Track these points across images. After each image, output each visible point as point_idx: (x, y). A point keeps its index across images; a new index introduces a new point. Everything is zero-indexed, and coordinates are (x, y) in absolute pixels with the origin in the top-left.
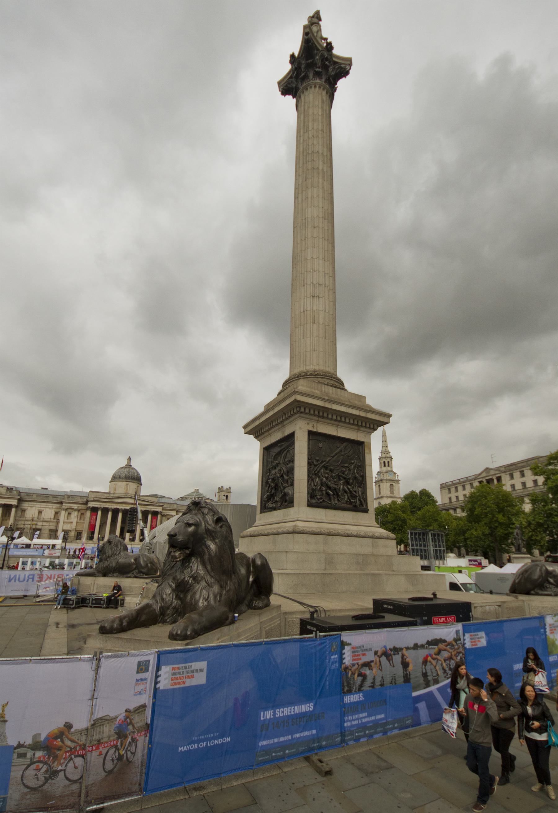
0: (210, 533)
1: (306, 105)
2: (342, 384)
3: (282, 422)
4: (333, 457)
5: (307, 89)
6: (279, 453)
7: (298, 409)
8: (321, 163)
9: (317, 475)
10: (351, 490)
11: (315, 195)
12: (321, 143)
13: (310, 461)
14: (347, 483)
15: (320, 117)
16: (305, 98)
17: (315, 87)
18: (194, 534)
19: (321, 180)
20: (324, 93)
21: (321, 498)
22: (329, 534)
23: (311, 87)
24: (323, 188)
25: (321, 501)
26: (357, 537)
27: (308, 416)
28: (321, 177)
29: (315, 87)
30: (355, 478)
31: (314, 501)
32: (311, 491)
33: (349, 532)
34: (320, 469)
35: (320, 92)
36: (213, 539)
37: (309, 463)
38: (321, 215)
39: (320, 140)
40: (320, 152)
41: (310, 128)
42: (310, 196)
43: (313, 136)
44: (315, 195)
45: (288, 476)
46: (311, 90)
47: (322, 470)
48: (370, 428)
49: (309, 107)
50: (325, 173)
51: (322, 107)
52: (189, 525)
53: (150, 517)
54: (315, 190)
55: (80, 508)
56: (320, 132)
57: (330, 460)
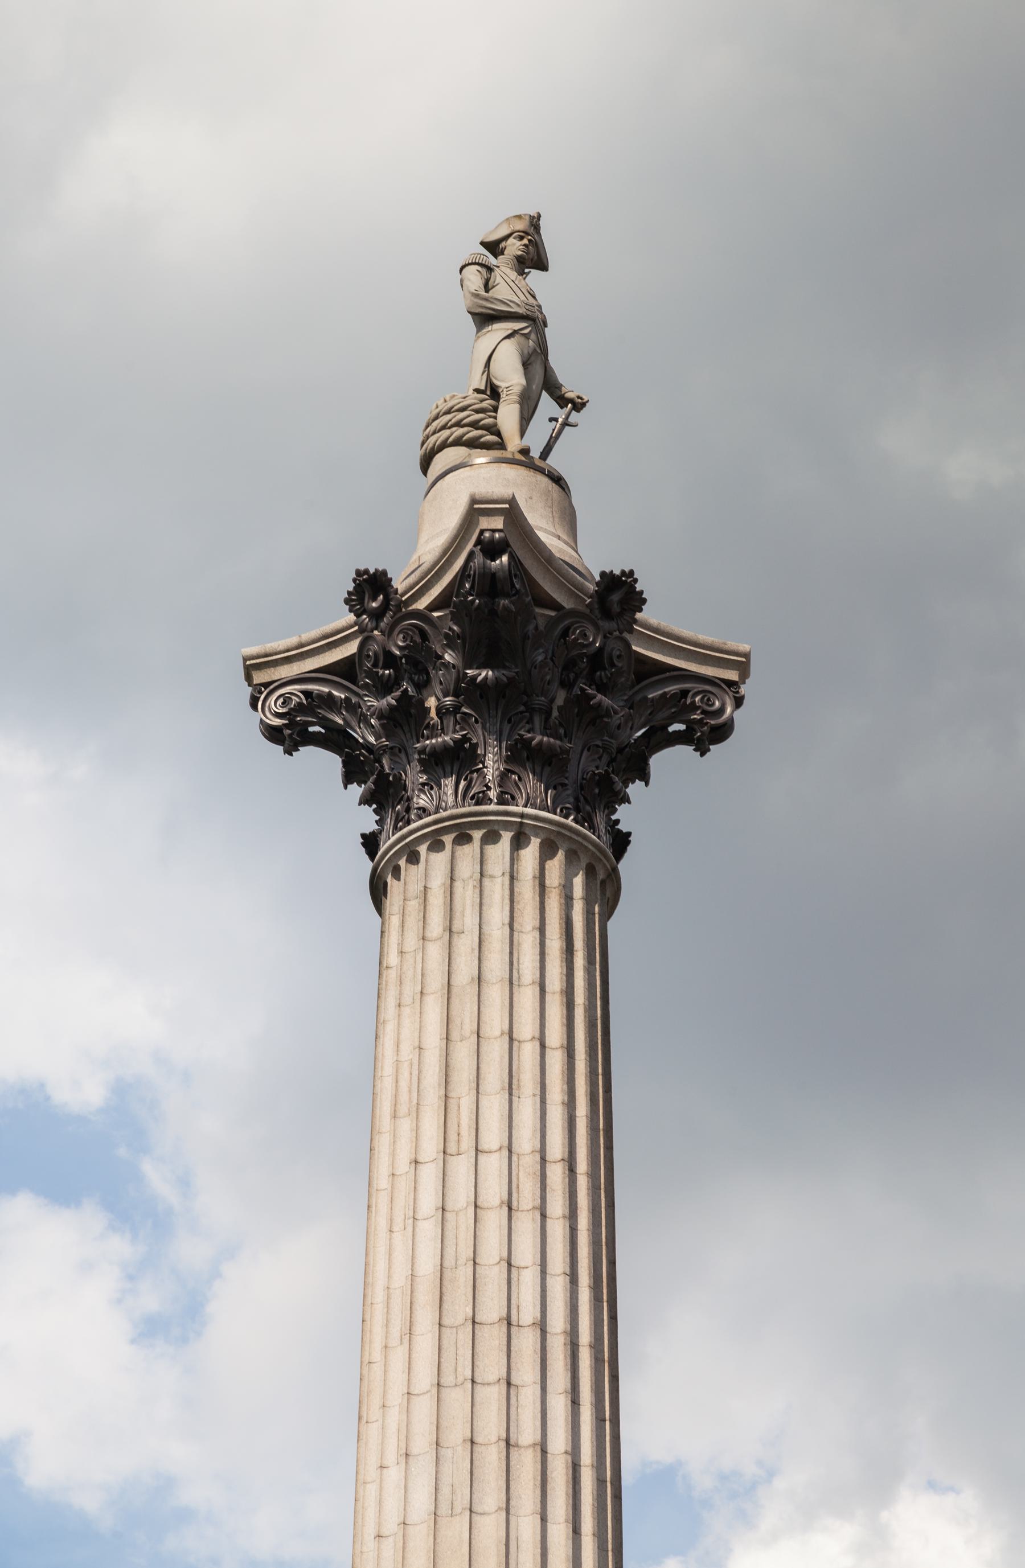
5: (463, 838)
17: (519, 842)
23: (492, 837)
29: (519, 842)
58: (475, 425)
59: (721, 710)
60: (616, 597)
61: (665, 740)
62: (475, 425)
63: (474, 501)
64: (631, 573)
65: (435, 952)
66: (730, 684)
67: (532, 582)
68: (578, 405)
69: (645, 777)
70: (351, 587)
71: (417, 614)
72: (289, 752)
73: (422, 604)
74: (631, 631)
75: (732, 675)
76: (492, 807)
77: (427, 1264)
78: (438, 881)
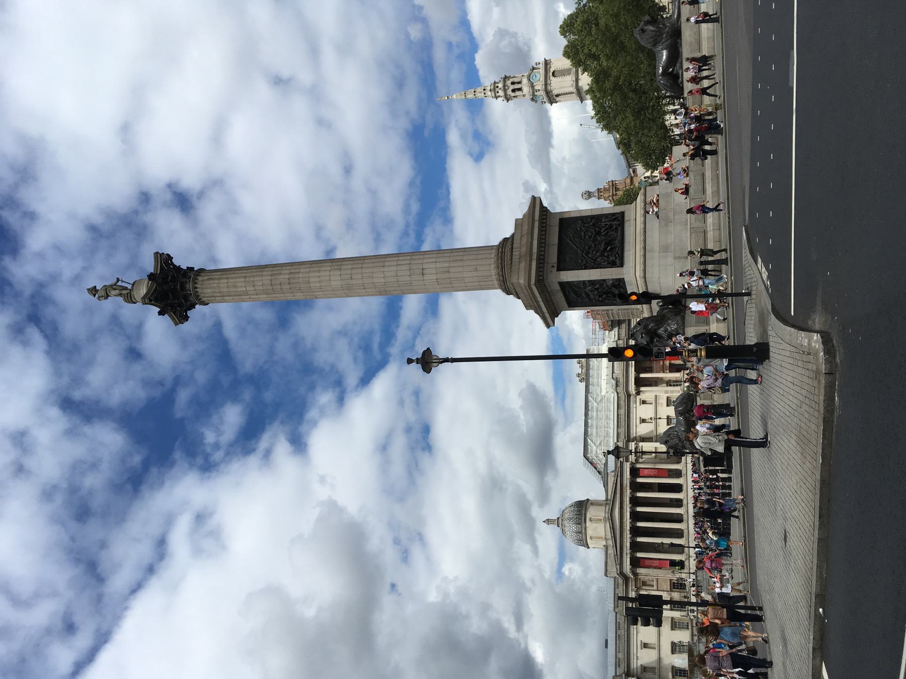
0: (645, 327)
1: (215, 295)
2: (505, 240)
3: (549, 293)
4: (577, 247)
5: (198, 296)
6: (576, 293)
7: (541, 281)
8: (282, 277)
9: (595, 260)
10: (605, 229)
11: (318, 280)
12: (260, 278)
13: (583, 268)
14: (599, 233)
15: (230, 280)
16: (207, 297)
17: (196, 288)
18: (646, 334)
19: (300, 276)
20: (200, 278)
21: (615, 255)
22: (645, 248)
23: (197, 292)
24: (308, 272)
25: (617, 256)
26: (646, 223)
27: (545, 272)
28: (297, 276)
29: (196, 288)
30: (594, 225)
31: (618, 262)
32: (609, 265)
33: (642, 230)
34: (589, 257)
35: (201, 282)
36: (648, 325)
37: (585, 269)
38: (338, 272)
39: (255, 279)
40: (269, 278)
41: (244, 289)
42: (319, 285)
43: (254, 286)
44: (318, 280)
45: (596, 285)
46: (199, 292)
47: (590, 256)
48: (546, 215)
49: (220, 292)
50: (291, 271)
51: (219, 279)
52: (642, 336)
53: (640, 480)
54: (311, 280)
55: (634, 587)
56: (247, 279)
57: (580, 249)
58: (128, 297)
60: (152, 278)
62: (128, 297)
63: (143, 304)
65: (217, 298)
66: (160, 255)
67: (154, 291)
68: (118, 280)
74: (157, 273)
75: (159, 255)
77: (265, 296)
78: (206, 299)
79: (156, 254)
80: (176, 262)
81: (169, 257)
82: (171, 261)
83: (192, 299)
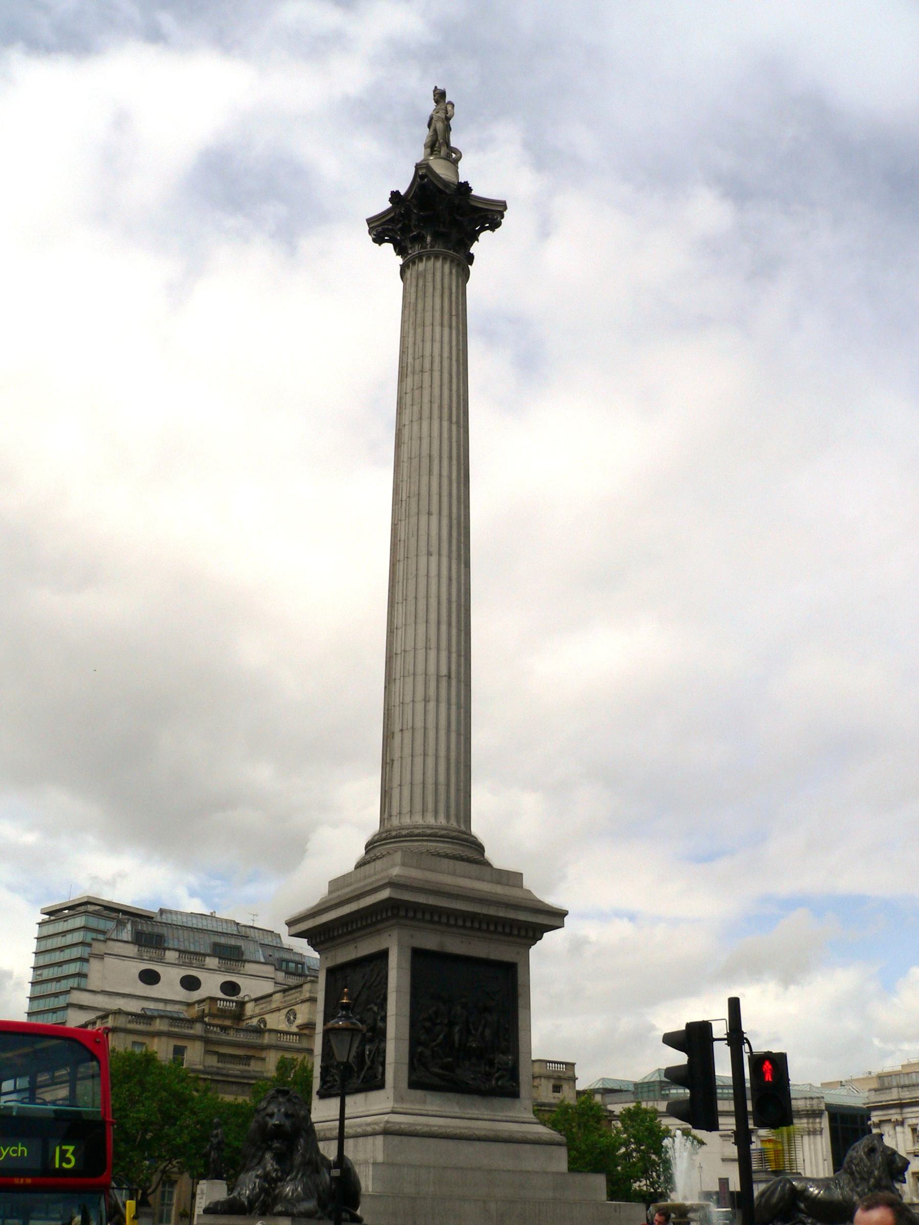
2: (480, 848)
59: (497, 219)
61: (483, 229)
64: (467, 182)
69: (478, 240)
70: (390, 196)
71: (408, 201)
72: (380, 245)
73: (409, 198)
76: (429, 249)
79: (503, 205)
80: (485, 236)
81: (495, 225)
82: (487, 229)
83: (415, 251)
